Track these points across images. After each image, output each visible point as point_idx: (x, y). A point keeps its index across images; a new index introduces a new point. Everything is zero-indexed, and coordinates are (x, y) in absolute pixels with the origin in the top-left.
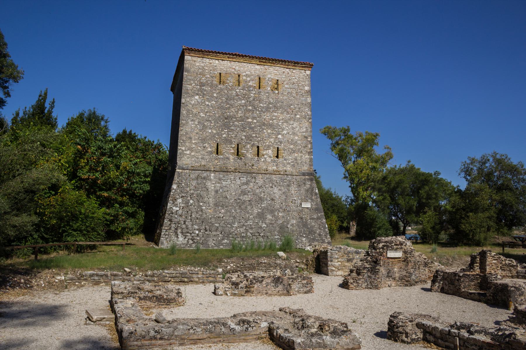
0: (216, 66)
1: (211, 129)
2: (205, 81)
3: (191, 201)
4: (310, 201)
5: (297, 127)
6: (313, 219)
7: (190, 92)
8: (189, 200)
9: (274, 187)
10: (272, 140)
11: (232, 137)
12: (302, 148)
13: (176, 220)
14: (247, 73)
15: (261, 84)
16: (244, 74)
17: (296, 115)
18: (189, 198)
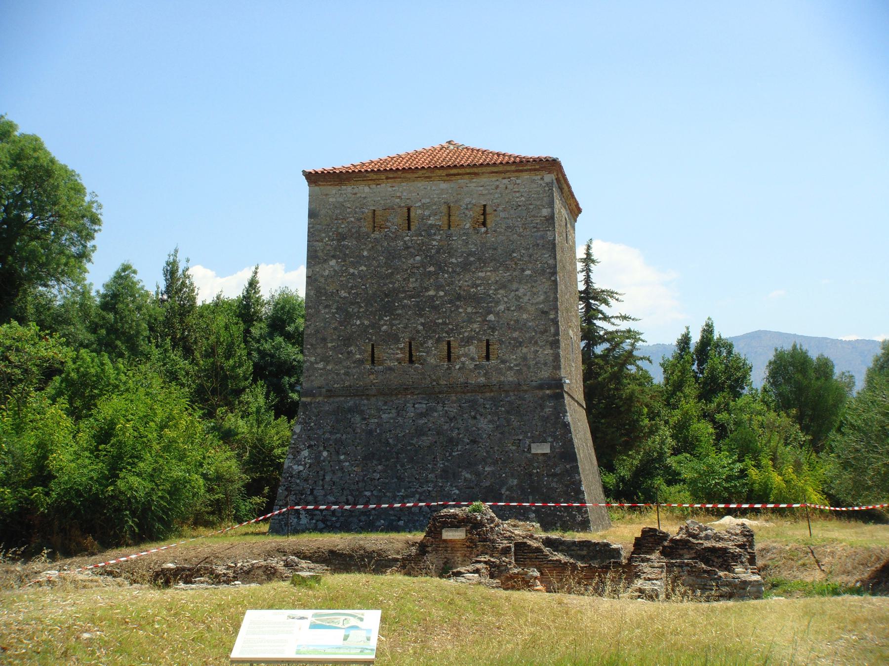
0: (365, 198)
1: (359, 318)
2: (345, 230)
3: (325, 454)
4: (550, 439)
5: (525, 295)
6: (554, 475)
7: (320, 254)
8: (320, 452)
9: (478, 417)
10: (475, 326)
11: (399, 329)
12: (539, 335)
13: (298, 488)
14: (423, 201)
15: (452, 218)
16: (419, 204)
17: (523, 270)
18: (321, 448)
